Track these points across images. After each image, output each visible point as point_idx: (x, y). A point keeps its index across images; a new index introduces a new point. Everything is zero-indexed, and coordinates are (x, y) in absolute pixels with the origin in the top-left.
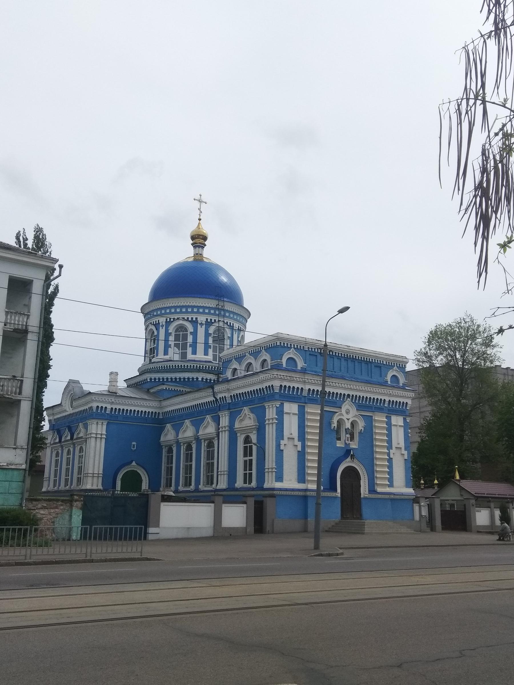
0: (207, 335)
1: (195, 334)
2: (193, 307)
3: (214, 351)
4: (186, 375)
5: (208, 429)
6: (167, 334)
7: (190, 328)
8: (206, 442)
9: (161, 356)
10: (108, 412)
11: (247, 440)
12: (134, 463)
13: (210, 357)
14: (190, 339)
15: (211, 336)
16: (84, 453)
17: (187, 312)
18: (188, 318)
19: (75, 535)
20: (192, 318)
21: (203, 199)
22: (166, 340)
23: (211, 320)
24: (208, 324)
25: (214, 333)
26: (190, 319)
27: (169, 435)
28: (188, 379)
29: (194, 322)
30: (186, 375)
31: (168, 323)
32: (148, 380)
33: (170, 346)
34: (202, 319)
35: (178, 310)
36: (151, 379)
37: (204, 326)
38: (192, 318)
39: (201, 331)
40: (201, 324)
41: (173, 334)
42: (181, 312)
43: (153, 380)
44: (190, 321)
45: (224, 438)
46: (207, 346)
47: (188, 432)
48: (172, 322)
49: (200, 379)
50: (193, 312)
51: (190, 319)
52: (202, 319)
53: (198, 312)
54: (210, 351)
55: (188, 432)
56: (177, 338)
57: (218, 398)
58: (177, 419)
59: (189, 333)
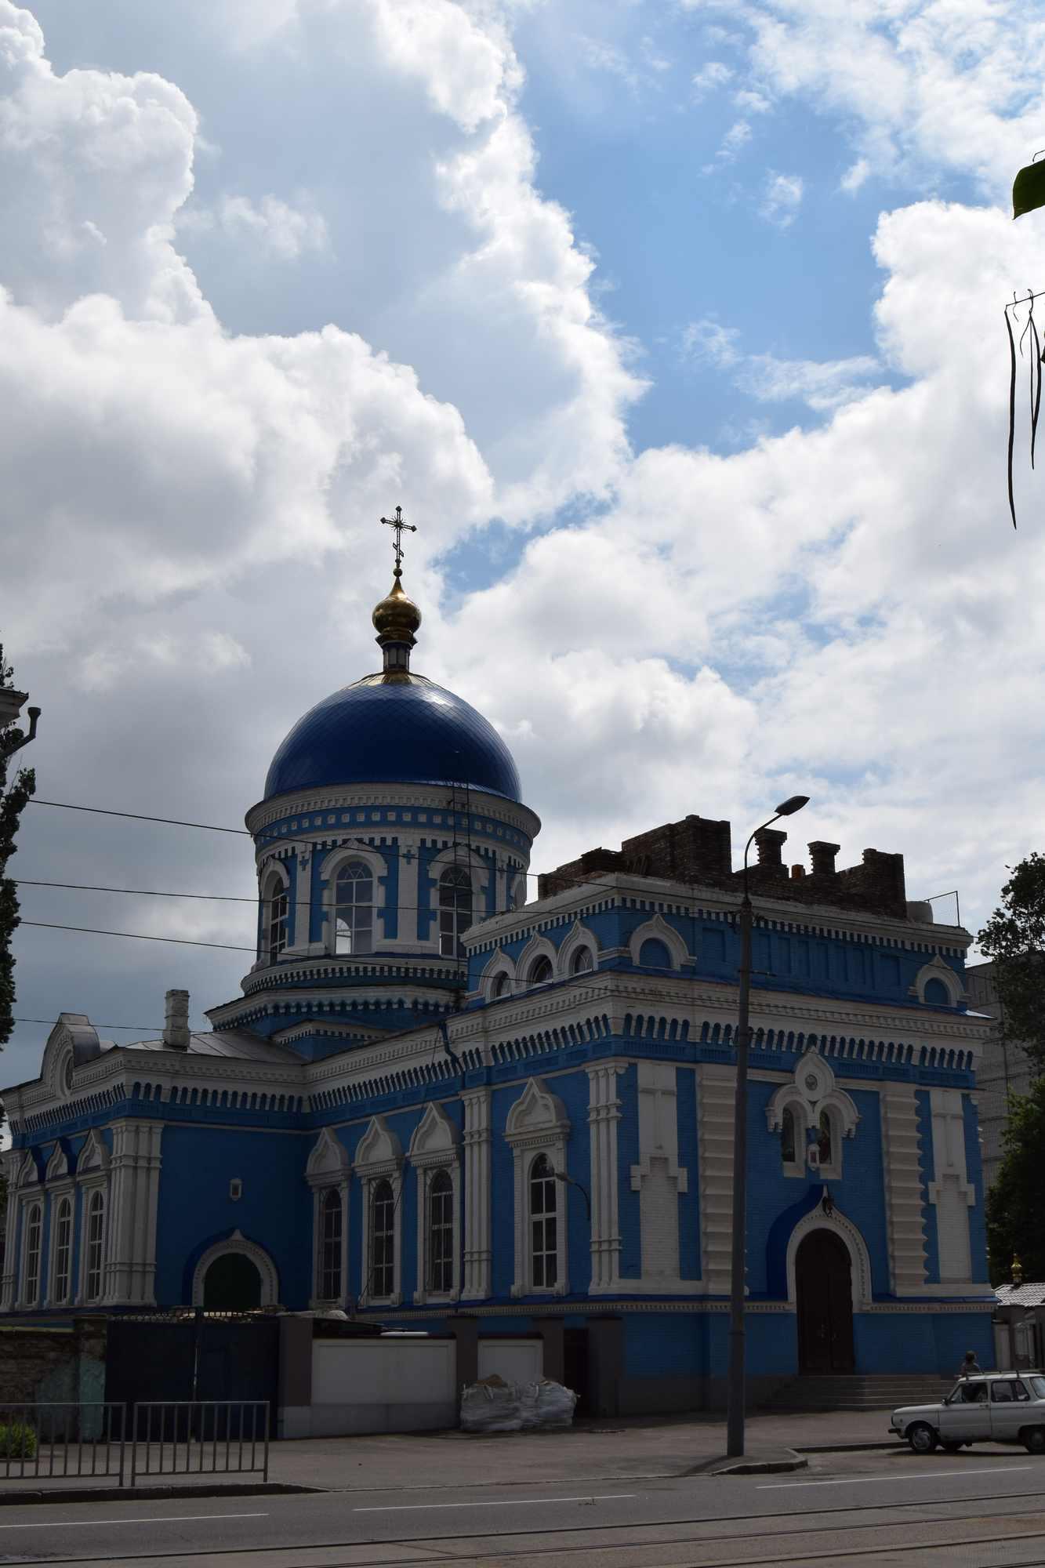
0: (424, 883)
1: (391, 882)
2: (384, 809)
3: (446, 925)
6: (317, 886)
7: (378, 866)
9: (301, 945)
13: (435, 944)
16: (104, 1211)
17: (369, 824)
18: (372, 840)
19: (90, 1426)
20: (383, 840)
21: (407, 519)
23: (434, 842)
24: (427, 854)
26: (377, 842)
29: (389, 852)
31: (320, 854)
36: (276, 1007)
37: (415, 862)
38: (383, 840)
39: (408, 874)
40: (409, 857)
41: (334, 883)
42: (353, 824)
46: (424, 915)
50: (384, 822)
51: (377, 842)
52: (409, 840)
53: (399, 823)
54: (435, 927)
56: (343, 894)
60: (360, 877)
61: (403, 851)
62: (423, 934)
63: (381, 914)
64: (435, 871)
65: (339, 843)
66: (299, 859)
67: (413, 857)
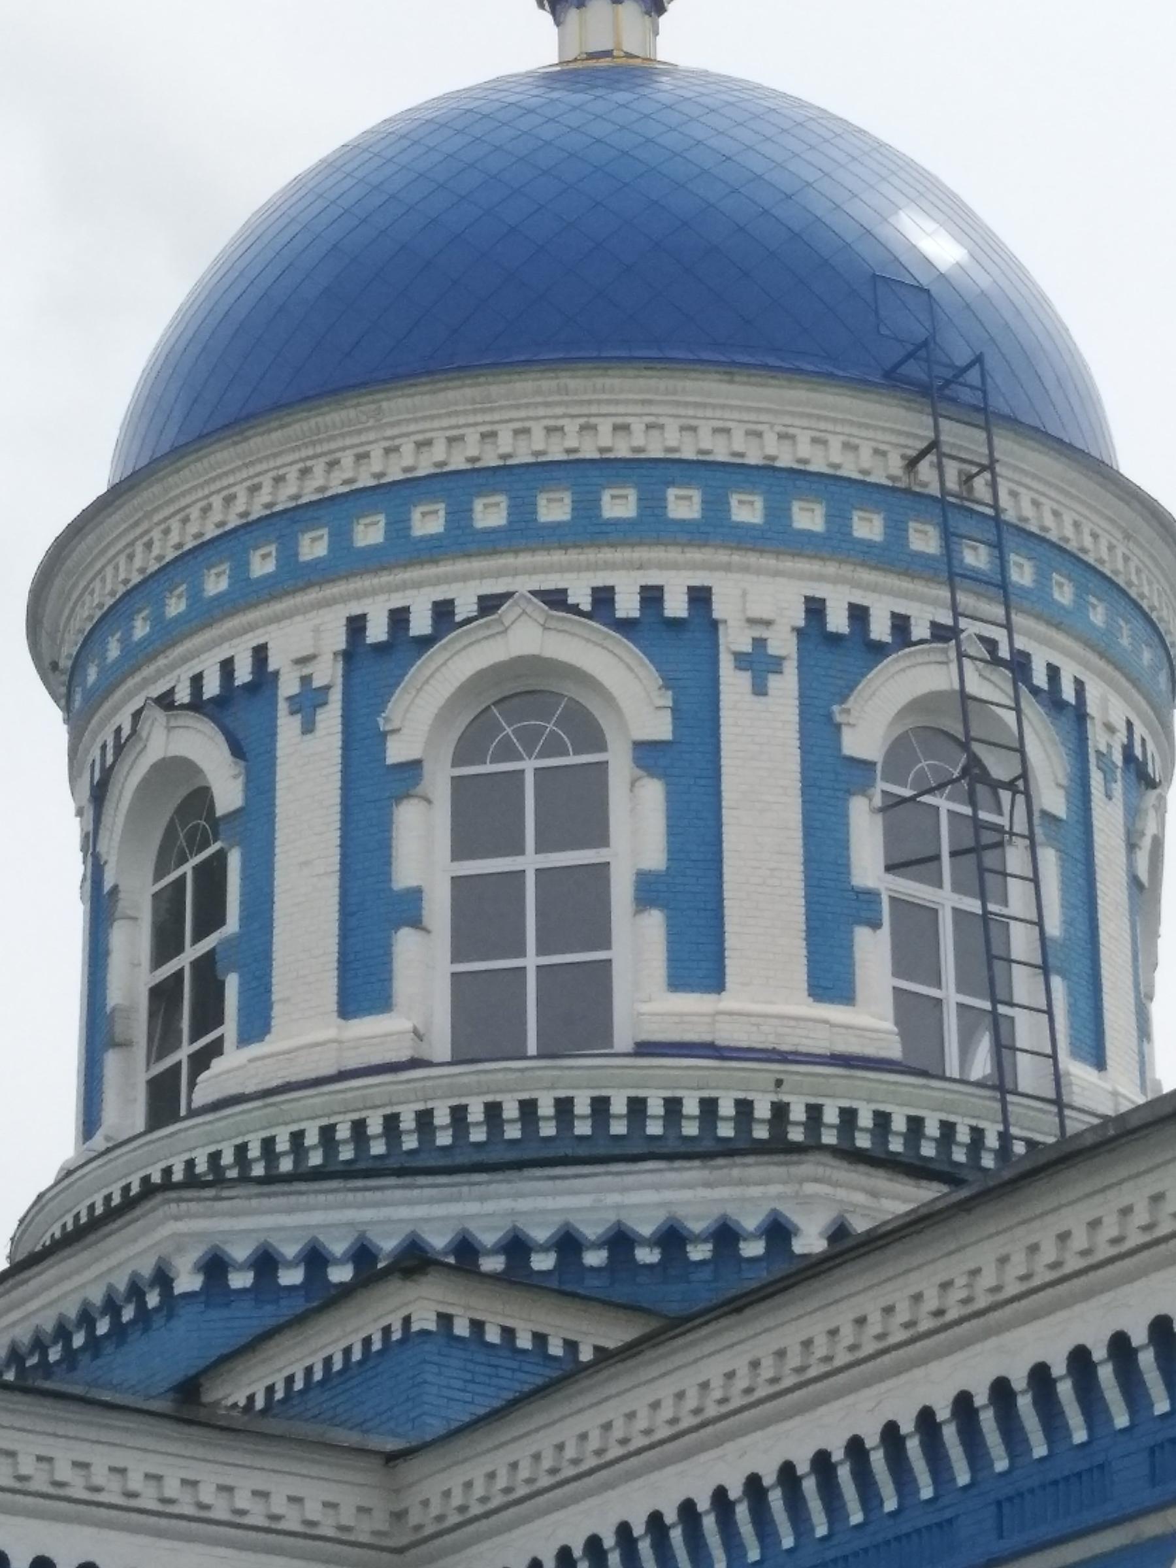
0: (828, 779)
1: (689, 764)
2: (653, 473)
3: (914, 952)
6: (371, 787)
7: (635, 698)
9: (305, 1028)
13: (868, 1020)
14: (638, 829)
15: (864, 789)
17: (589, 530)
18: (604, 598)
20: (652, 597)
23: (859, 614)
24: (838, 653)
25: (900, 753)
26: (627, 605)
29: (679, 638)
31: (376, 661)
32: (187, 1281)
33: (408, 910)
34: (759, 600)
35: (490, 513)
36: (215, 1266)
37: (786, 686)
38: (652, 597)
39: (759, 736)
40: (759, 664)
41: (439, 781)
42: (523, 533)
43: (240, 1280)
44: (626, 626)
46: (832, 911)
48: (425, 643)
50: (651, 527)
51: (627, 605)
52: (759, 600)
53: (713, 530)
54: (873, 951)
56: (482, 819)
59: (619, 761)
60: (554, 748)
61: (735, 638)
62: (830, 979)
63: (649, 892)
64: (867, 730)
65: (465, 607)
66: (289, 686)
67: (776, 665)
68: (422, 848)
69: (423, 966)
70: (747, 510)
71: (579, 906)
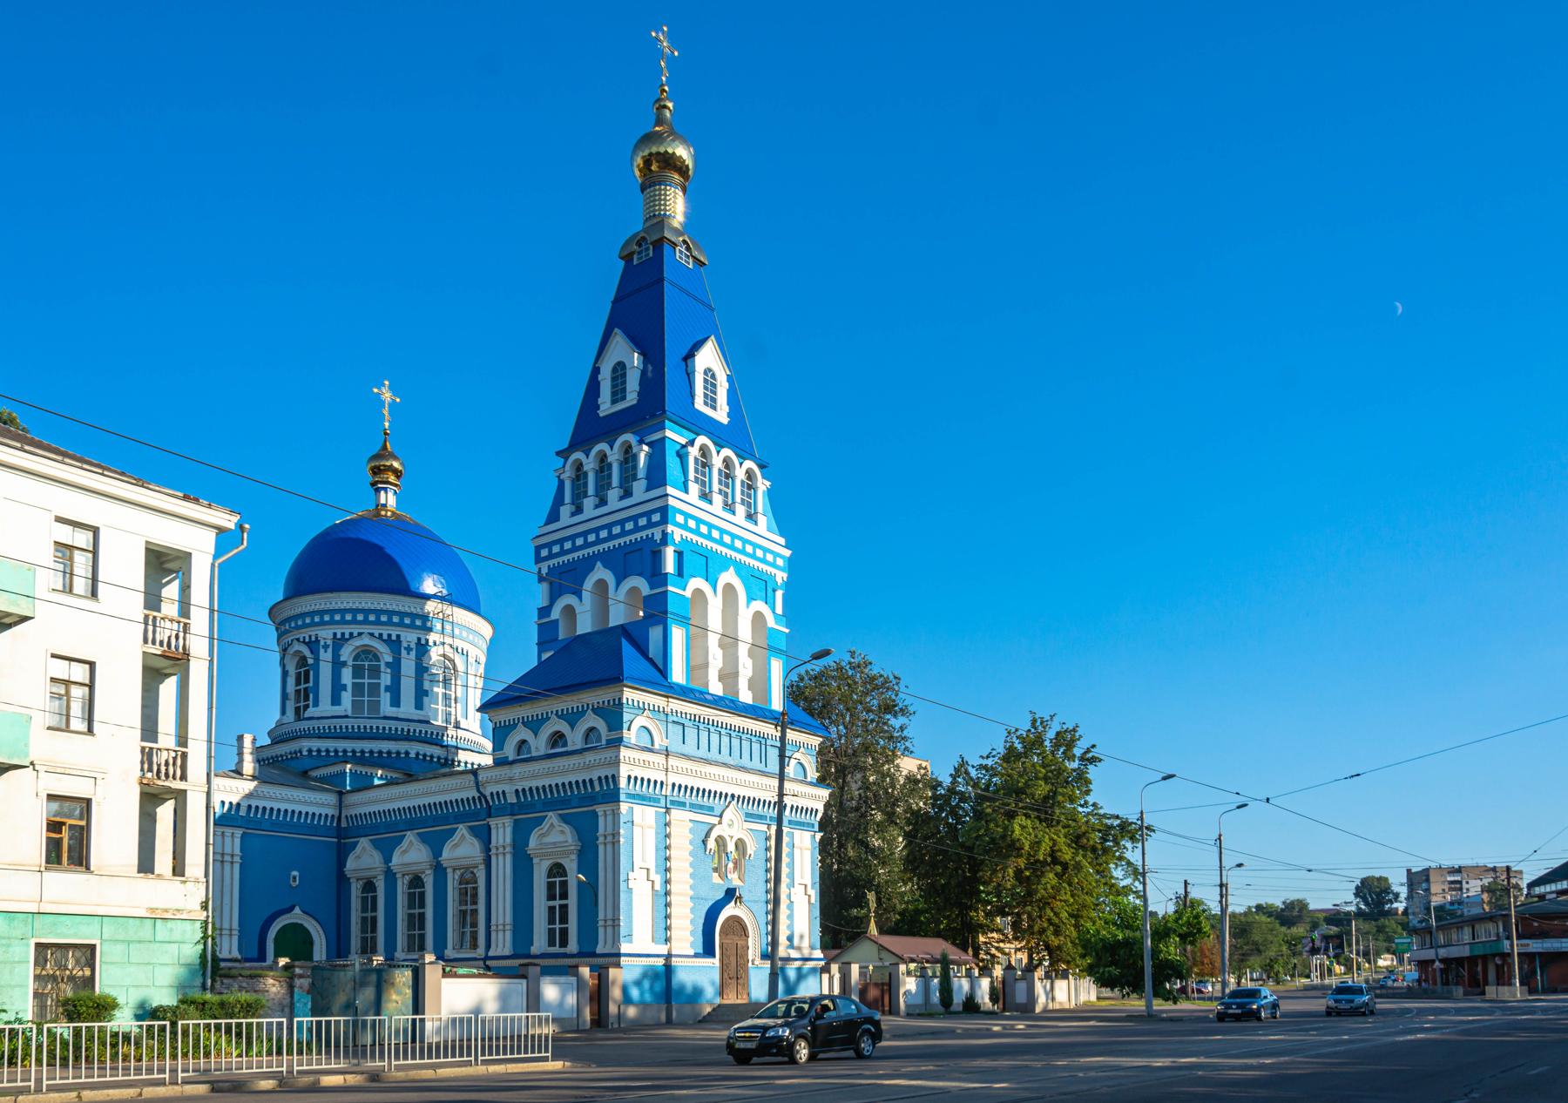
4: (385, 746)
5: (462, 848)
6: (338, 665)
8: (458, 873)
9: (325, 707)
10: (243, 813)
11: (557, 870)
12: (297, 910)
17: (378, 623)
22: (336, 676)
27: (364, 859)
28: (389, 753)
29: (395, 644)
30: (385, 746)
31: (339, 642)
33: (344, 687)
36: (310, 751)
42: (366, 622)
45: (503, 867)
47: (412, 854)
49: (413, 755)
53: (401, 624)
55: (412, 854)
56: (358, 672)
57: (488, 794)
58: (387, 832)
68: (347, 676)
69: (347, 698)
70: (407, 621)
71: (374, 689)
